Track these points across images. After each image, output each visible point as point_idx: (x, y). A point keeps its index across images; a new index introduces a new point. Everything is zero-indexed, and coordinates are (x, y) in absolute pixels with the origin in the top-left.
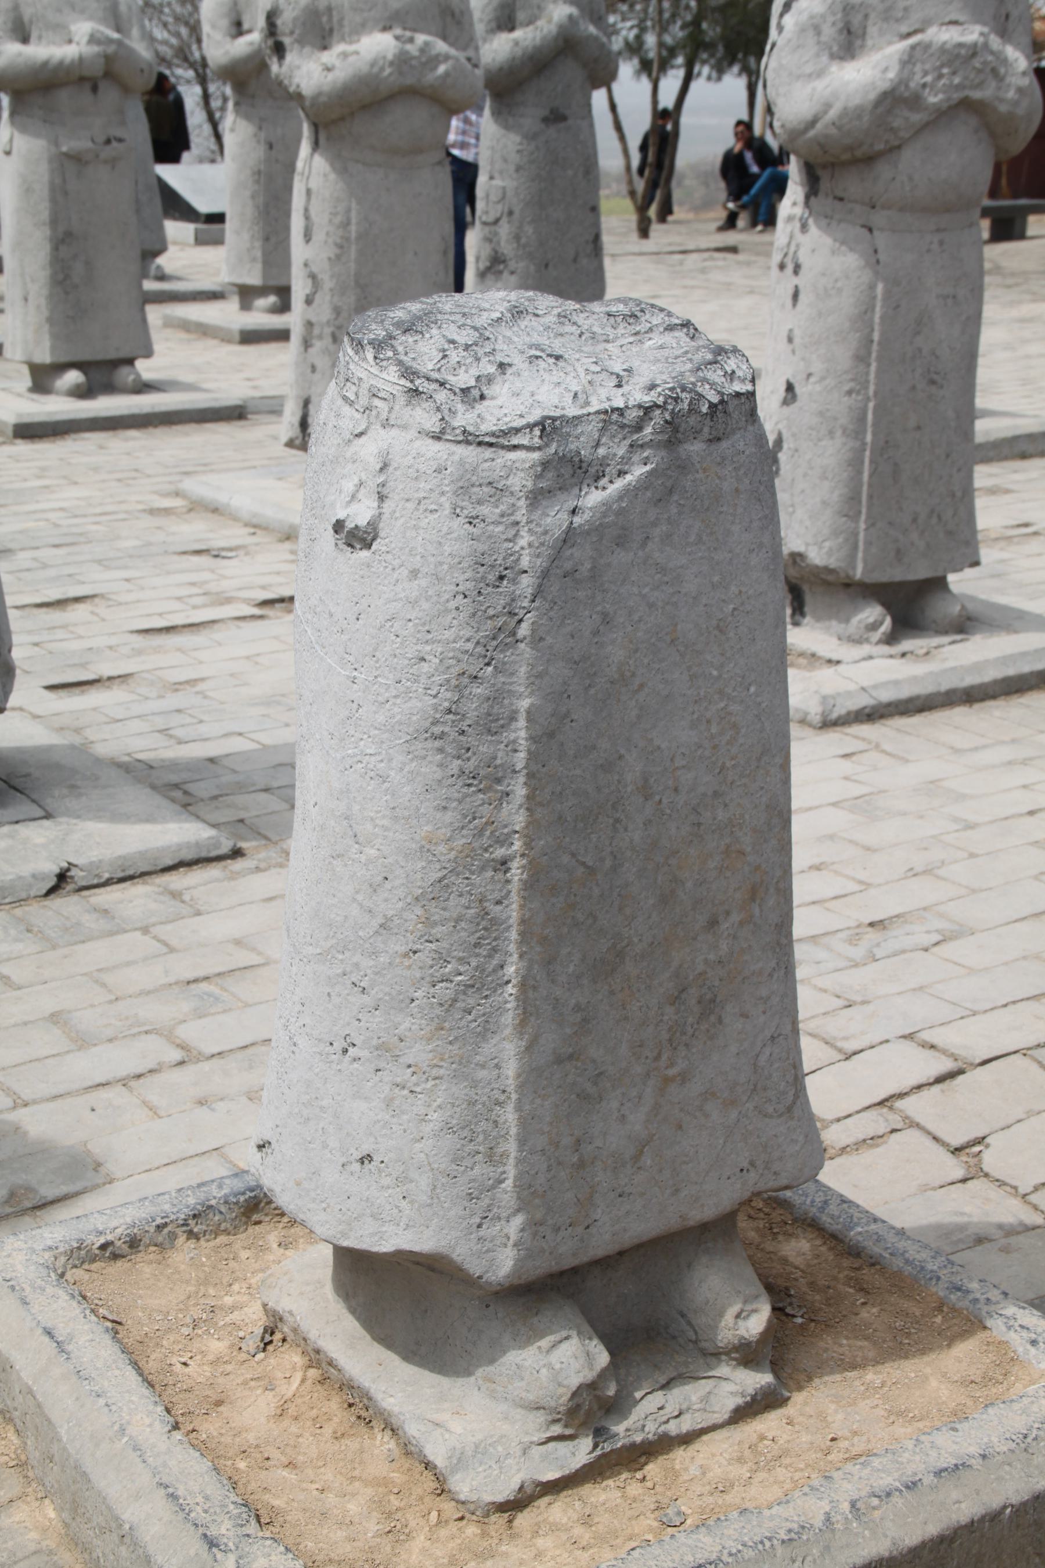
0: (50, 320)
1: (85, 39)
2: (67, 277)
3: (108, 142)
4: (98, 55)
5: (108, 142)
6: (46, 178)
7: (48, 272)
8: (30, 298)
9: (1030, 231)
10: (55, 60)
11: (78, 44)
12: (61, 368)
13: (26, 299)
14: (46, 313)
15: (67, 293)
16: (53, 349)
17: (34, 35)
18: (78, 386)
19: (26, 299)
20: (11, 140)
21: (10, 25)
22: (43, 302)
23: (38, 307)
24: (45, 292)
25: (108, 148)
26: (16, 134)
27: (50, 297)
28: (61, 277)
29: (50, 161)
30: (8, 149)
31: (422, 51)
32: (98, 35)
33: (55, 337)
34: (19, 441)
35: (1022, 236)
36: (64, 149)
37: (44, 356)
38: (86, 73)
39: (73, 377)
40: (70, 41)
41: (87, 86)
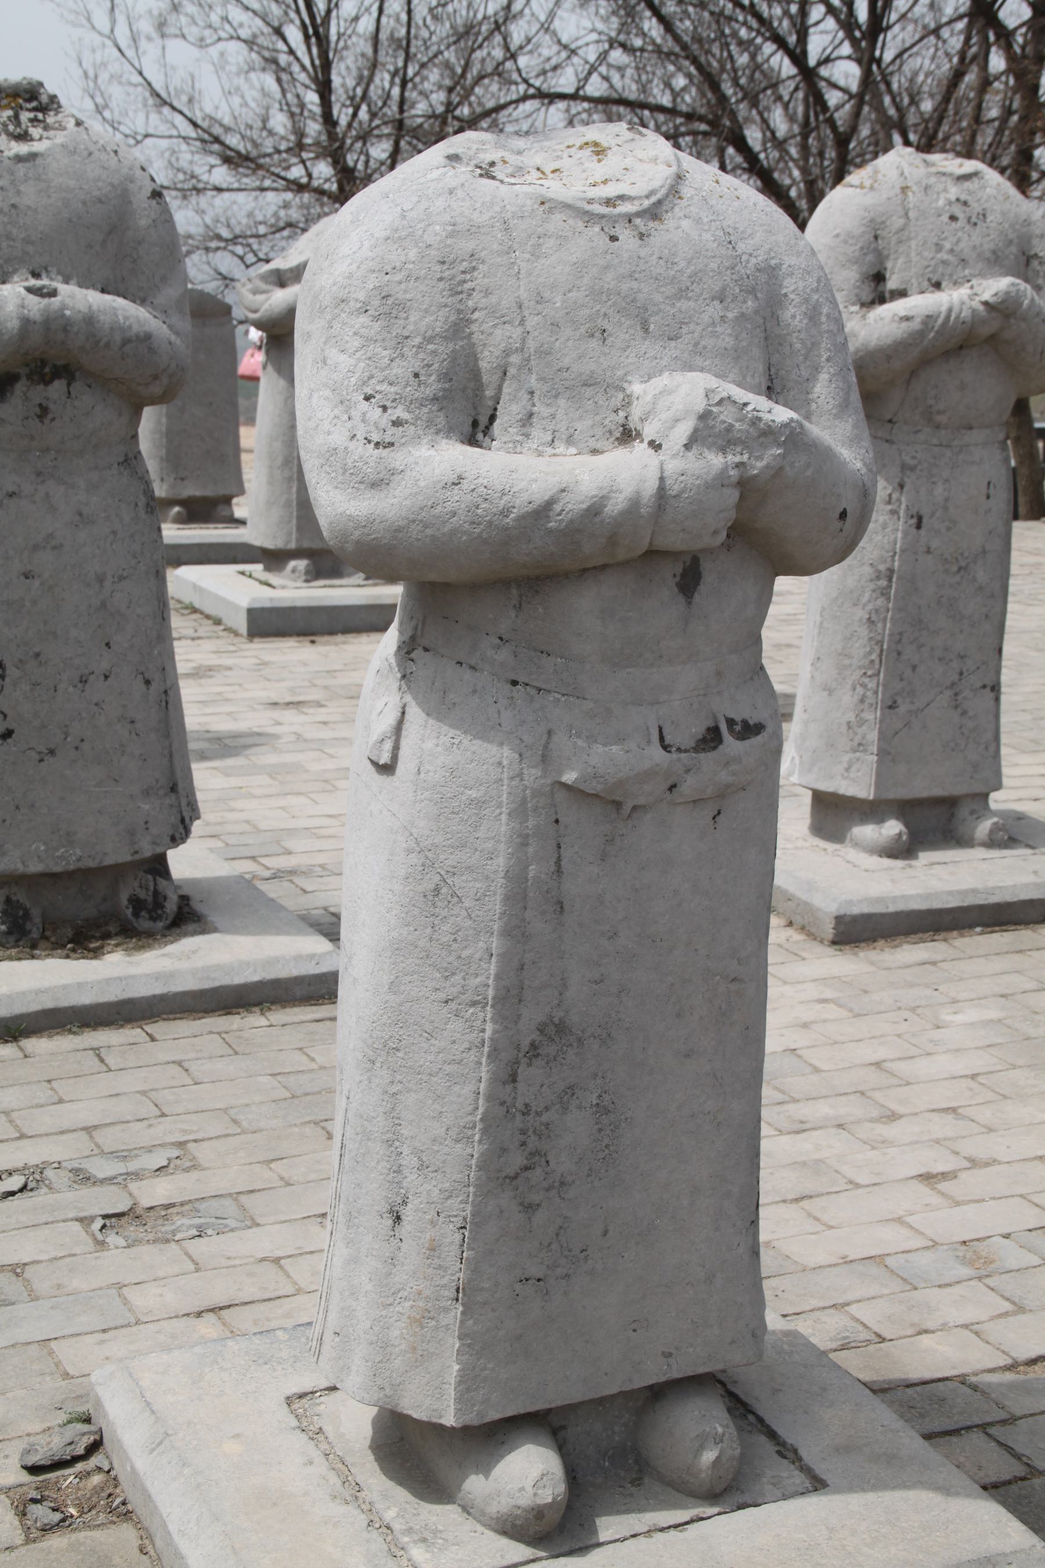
1: (683, 431)
2: (536, 1158)
3: (711, 739)
4: (720, 481)
5: (711, 739)
6: (501, 862)
8: (408, 1214)
10: (574, 504)
11: (655, 446)
14: (456, 1273)
15: (529, 1208)
16: (467, 1382)
17: (509, 412)
20: (398, 729)
21: (432, 386)
24: (461, 1208)
25: (707, 758)
26: (415, 714)
28: (517, 1160)
29: (520, 811)
30: (385, 758)
32: (727, 415)
36: (570, 777)
38: (673, 540)
40: (627, 435)
41: (670, 573)
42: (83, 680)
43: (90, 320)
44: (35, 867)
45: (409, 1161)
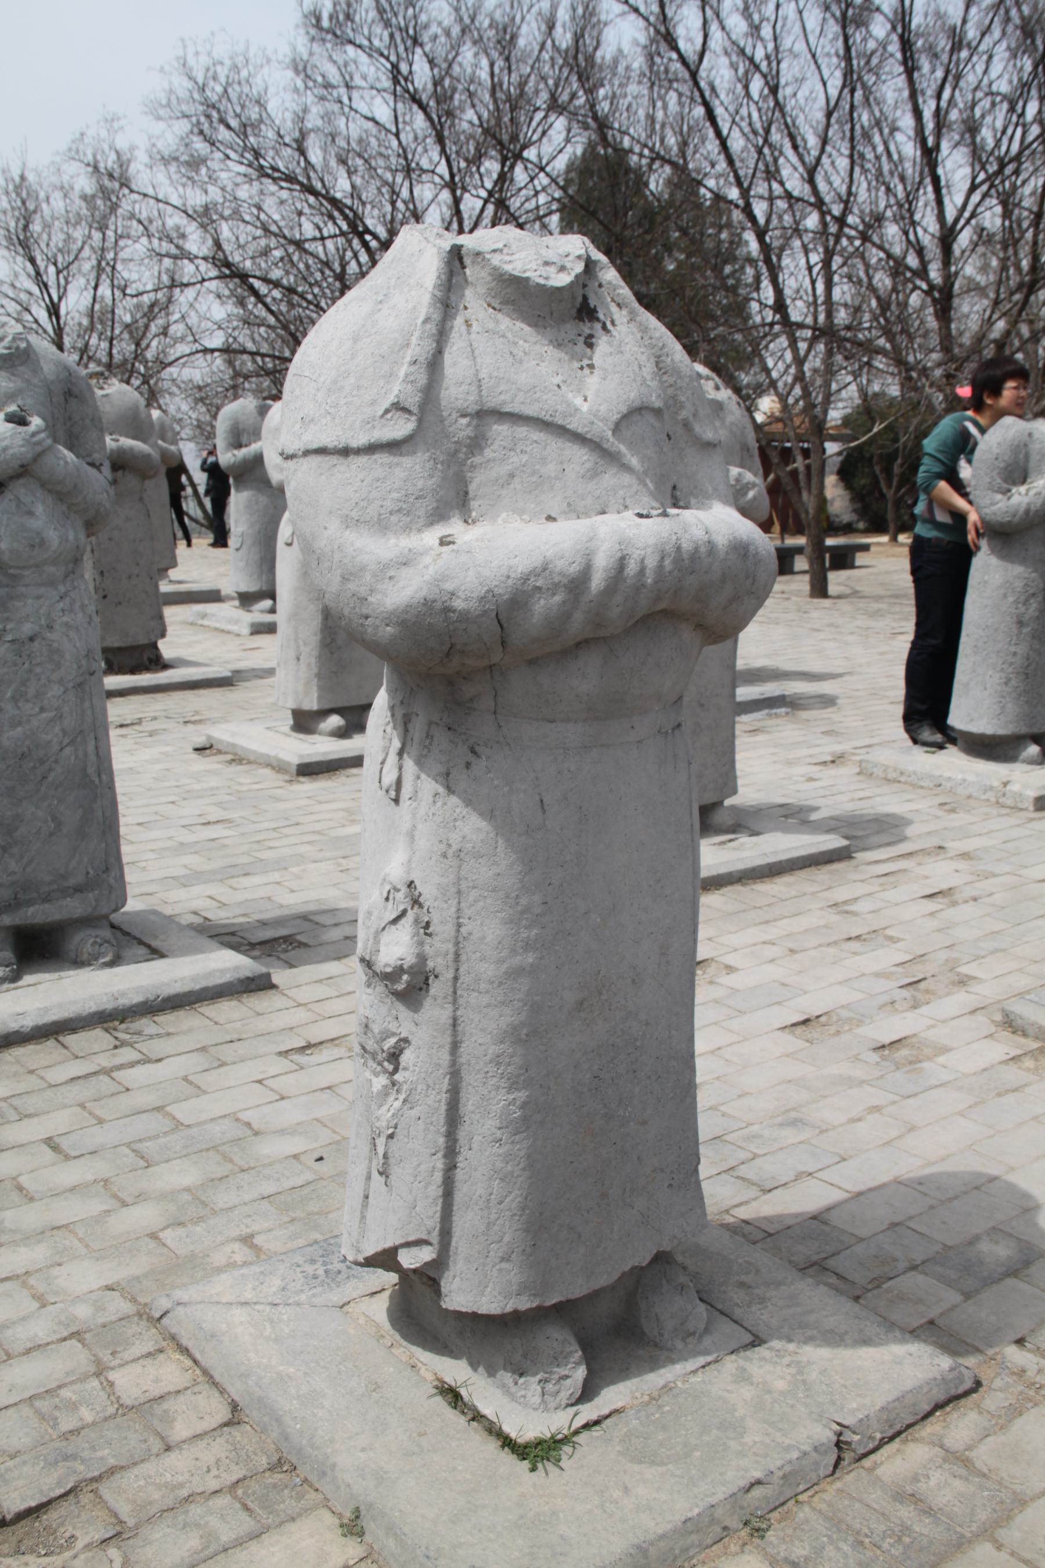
0: (319, 676)
2: (333, 640)
7: (319, 637)
9: (857, 563)
12: (324, 713)
13: (298, 659)
14: (315, 670)
16: (320, 698)
18: (339, 728)
19: (298, 659)
22: (313, 661)
23: (309, 665)
24: (315, 653)
27: (320, 657)
28: (329, 641)
31: (737, 480)
33: (321, 689)
34: (302, 779)
35: (852, 566)
37: (312, 704)
39: (335, 721)
42: (130, 577)
43: (131, 449)
44: (116, 645)
45: (301, 643)
